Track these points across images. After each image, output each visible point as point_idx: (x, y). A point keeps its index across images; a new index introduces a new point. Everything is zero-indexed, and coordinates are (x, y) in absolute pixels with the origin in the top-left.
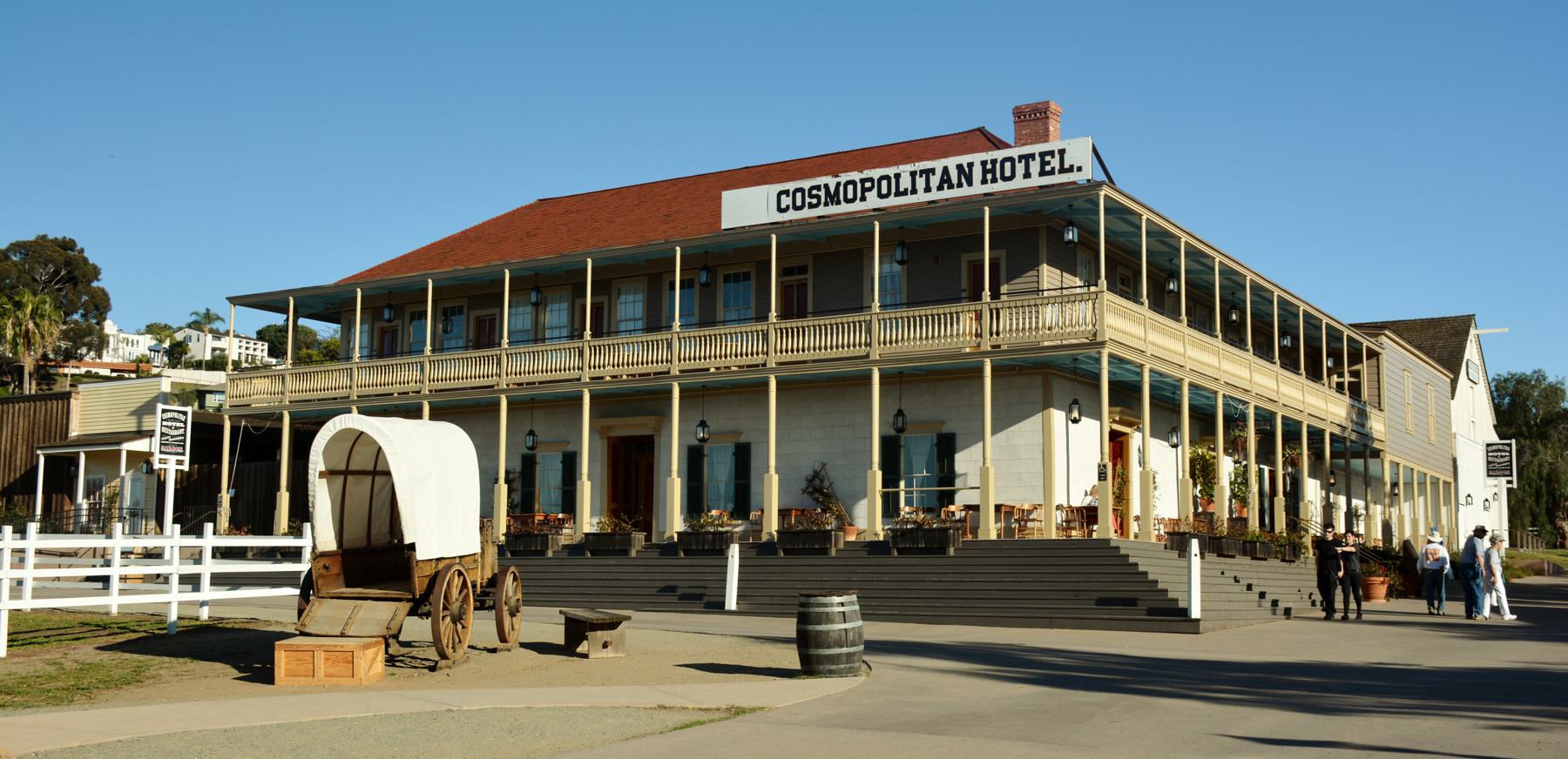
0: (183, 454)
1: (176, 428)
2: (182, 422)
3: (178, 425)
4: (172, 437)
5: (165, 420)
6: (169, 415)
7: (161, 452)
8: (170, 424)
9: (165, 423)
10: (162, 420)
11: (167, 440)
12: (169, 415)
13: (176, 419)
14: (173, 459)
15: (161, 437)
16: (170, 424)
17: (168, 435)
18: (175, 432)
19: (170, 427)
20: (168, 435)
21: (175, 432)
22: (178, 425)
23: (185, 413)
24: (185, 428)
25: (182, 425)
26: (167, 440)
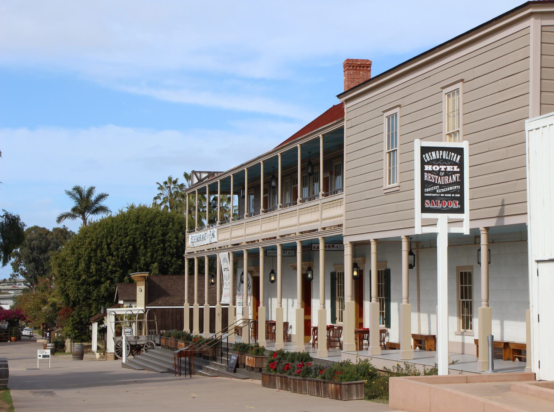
0: (461, 210)
1: (447, 173)
2: (454, 164)
3: (449, 168)
4: (441, 186)
5: (428, 163)
6: (434, 155)
7: (424, 210)
8: (436, 168)
9: (428, 168)
10: (423, 163)
11: (435, 192)
12: (434, 155)
13: (445, 160)
14: (443, 218)
15: (423, 187)
16: (436, 168)
17: (434, 184)
18: (447, 180)
19: (438, 173)
20: (434, 184)
21: (447, 180)
22: (449, 168)
23: (459, 151)
24: (462, 172)
25: (456, 169)
26: (435, 192)
